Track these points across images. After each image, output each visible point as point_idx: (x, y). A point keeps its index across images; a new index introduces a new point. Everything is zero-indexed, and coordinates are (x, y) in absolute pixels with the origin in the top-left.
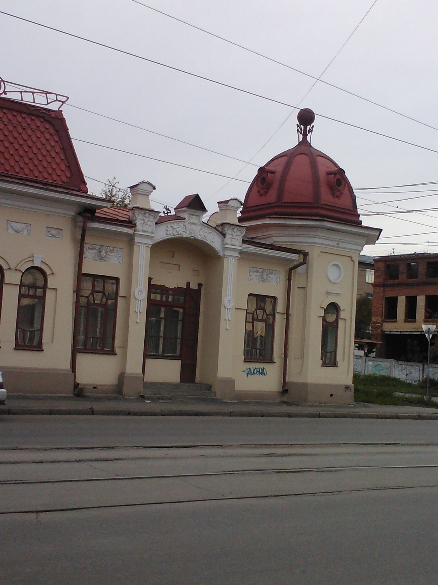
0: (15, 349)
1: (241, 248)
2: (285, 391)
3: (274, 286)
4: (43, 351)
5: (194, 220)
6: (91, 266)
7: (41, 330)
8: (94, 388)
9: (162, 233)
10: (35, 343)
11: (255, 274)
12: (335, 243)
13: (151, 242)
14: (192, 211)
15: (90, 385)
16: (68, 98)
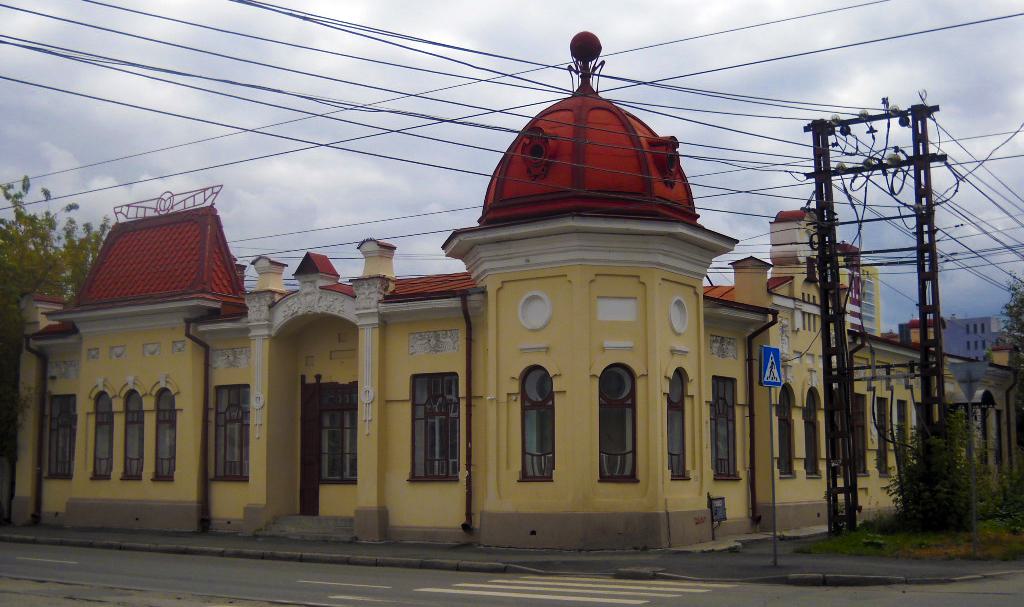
0: (92, 479)
1: (376, 310)
2: (466, 527)
3: (450, 359)
4: (638, 481)
5: (308, 289)
6: (224, 376)
7: (634, 451)
8: (229, 523)
9: (281, 316)
10: (627, 472)
11: (419, 342)
12: (521, 261)
13: (273, 333)
14: (303, 278)
15: (223, 520)
16: (222, 186)
